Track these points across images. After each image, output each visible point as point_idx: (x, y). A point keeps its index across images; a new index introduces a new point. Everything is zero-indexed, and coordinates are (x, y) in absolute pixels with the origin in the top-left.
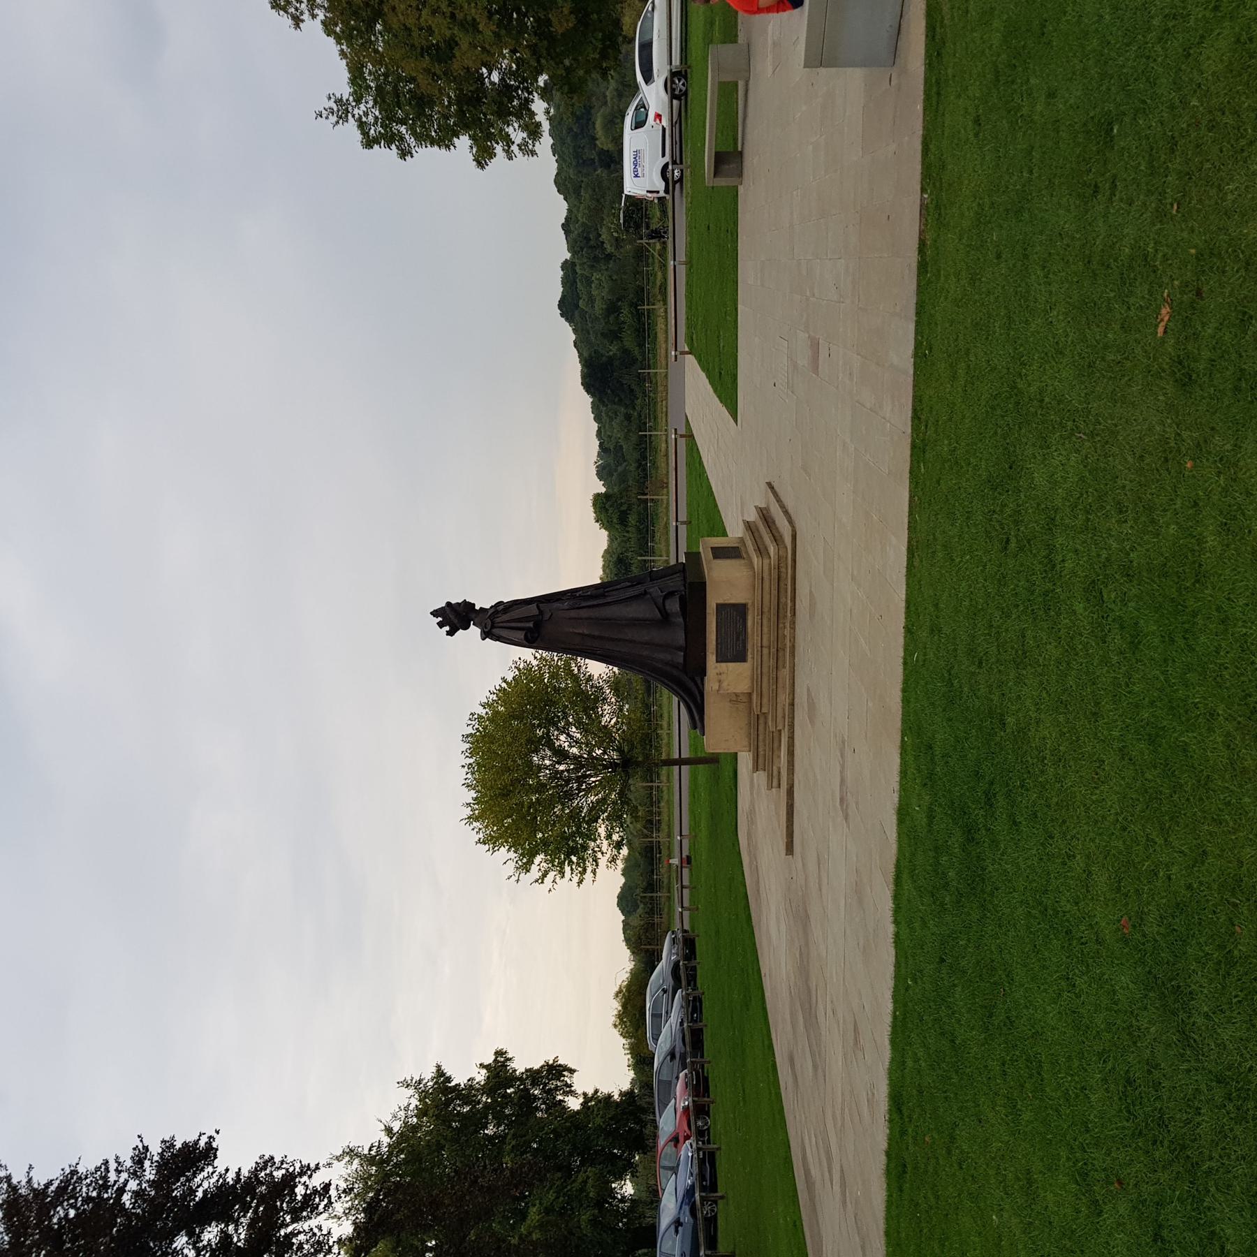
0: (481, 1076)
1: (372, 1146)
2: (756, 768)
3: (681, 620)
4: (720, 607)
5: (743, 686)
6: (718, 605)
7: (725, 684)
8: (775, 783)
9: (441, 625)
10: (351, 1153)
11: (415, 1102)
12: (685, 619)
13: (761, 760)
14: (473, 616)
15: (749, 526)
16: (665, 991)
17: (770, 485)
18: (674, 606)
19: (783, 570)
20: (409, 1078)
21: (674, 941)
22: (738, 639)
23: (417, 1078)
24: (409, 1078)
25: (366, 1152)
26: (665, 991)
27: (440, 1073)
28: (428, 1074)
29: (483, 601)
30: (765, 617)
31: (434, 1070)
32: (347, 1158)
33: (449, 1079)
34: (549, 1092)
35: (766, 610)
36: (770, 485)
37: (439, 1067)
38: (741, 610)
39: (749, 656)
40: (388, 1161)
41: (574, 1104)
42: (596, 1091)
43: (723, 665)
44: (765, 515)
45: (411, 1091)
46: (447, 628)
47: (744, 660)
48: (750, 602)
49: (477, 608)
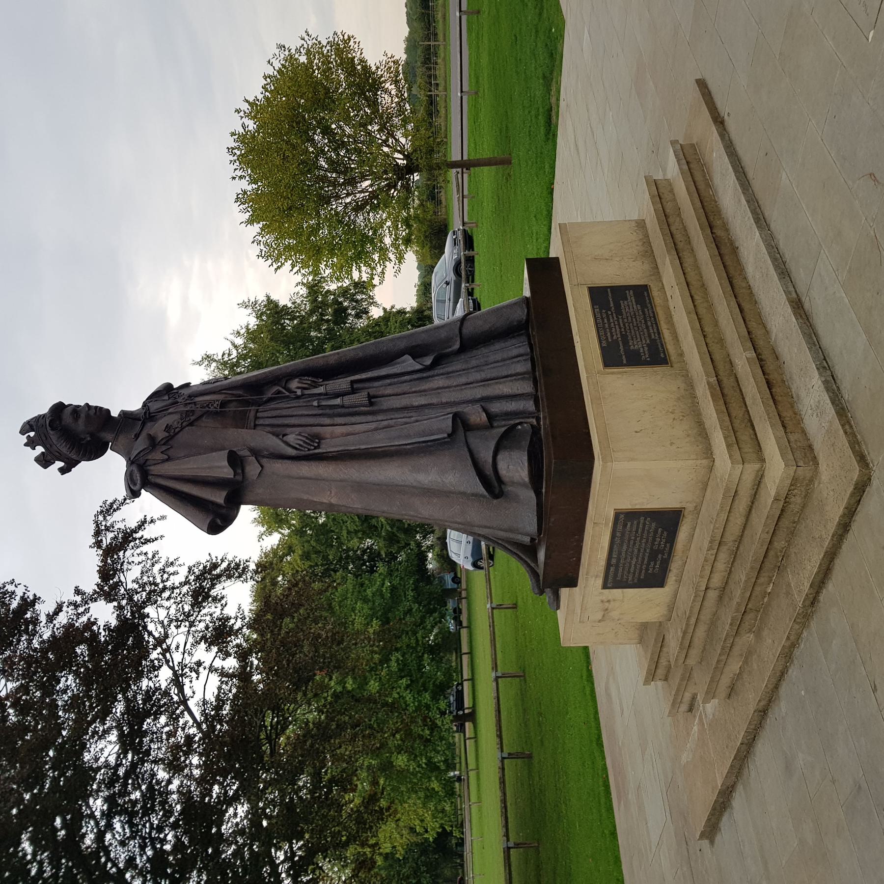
0: (304, 291)
1: (224, 354)
2: (651, 676)
3: (532, 494)
4: (626, 519)
5: (653, 615)
6: (617, 515)
7: (615, 614)
8: (684, 707)
9: (44, 461)
10: (208, 358)
11: (253, 322)
12: (538, 493)
13: (661, 672)
14: (108, 436)
15: (660, 193)
16: (447, 283)
17: (702, 84)
18: (515, 467)
19: (797, 500)
20: (246, 300)
21: (455, 242)
22: (653, 556)
23: (252, 300)
24: (246, 300)
25: (220, 357)
26: (447, 283)
27: (268, 297)
28: (262, 298)
29: (125, 397)
30: (724, 548)
31: (265, 299)
32: (206, 363)
33: (276, 305)
34: (357, 301)
35: (730, 537)
36: (702, 84)
37: (268, 297)
38: (668, 521)
39: (671, 579)
40: (237, 364)
41: (376, 313)
42: (393, 307)
43: (617, 593)
44: (691, 159)
45: (250, 311)
46: (59, 464)
47: (661, 584)
48: (690, 507)
49: (115, 413)
